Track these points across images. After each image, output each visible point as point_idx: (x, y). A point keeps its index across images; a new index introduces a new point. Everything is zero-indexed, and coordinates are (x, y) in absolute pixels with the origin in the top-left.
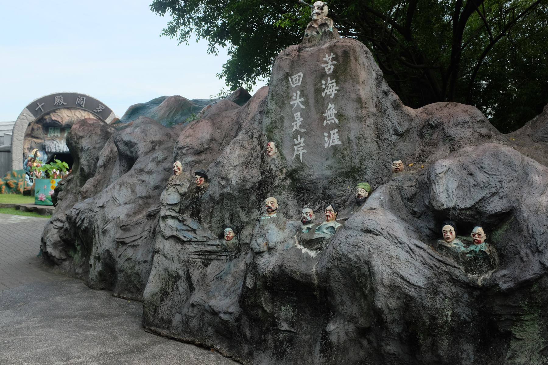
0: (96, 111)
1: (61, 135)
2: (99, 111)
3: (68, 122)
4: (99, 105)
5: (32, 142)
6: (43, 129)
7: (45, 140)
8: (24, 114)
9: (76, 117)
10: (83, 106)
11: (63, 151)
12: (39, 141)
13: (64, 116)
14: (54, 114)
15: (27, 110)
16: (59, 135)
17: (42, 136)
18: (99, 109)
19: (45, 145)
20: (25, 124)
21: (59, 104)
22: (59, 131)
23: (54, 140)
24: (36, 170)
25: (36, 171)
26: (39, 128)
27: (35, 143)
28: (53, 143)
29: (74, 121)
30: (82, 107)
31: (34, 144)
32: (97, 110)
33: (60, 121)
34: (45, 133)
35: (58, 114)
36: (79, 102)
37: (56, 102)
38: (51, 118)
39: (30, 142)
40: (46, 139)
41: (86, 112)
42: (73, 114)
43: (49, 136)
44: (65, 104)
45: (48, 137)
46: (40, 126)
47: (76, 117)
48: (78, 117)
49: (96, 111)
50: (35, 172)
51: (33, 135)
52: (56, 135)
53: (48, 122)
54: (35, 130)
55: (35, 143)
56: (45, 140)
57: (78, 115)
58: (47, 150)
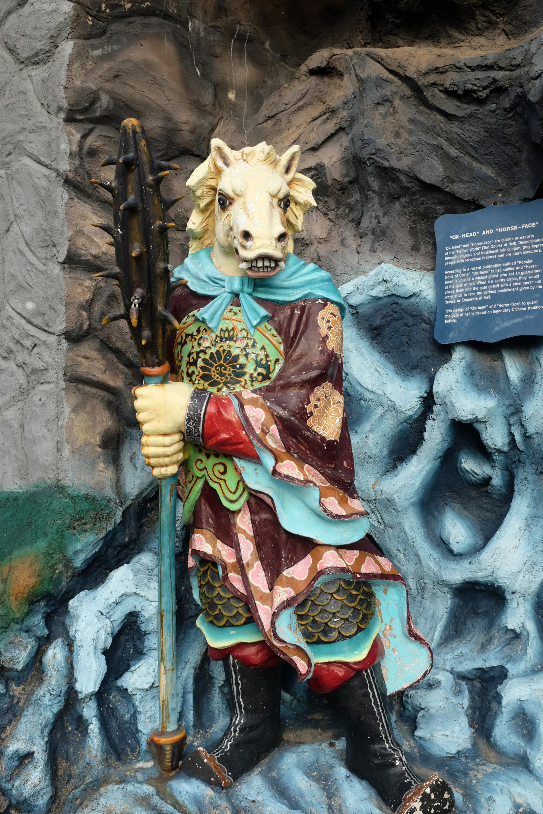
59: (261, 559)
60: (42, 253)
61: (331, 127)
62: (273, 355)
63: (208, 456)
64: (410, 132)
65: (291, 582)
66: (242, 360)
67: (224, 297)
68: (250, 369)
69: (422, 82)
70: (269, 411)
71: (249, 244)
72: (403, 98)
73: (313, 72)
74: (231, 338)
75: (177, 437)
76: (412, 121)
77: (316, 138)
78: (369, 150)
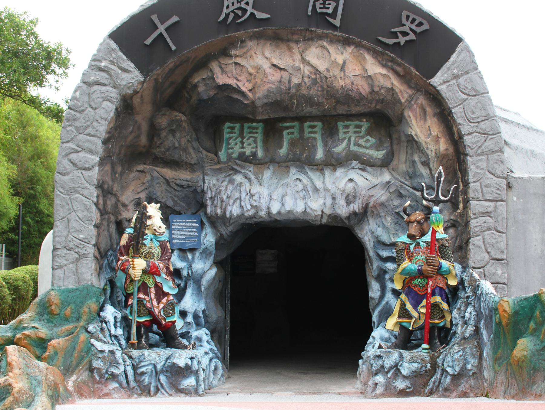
0: (391, 41)
1: (266, 149)
2: (402, 40)
3: (279, 89)
4: (405, 13)
5: (153, 178)
6: (196, 130)
7: (204, 174)
8: (103, 64)
9: (307, 70)
10: (337, 22)
11: (269, 213)
12: (183, 176)
13: (258, 68)
14: (225, 61)
15: (114, 46)
16: (260, 153)
17: (193, 157)
18: (405, 34)
19: (203, 192)
20: (106, 104)
21: (237, 17)
22: (259, 136)
23: (236, 172)
24: (144, 288)
25: (147, 293)
26: (179, 123)
27: (168, 182)
28: (231, 181)
29: (299, 85)
30: (334, 27)
31: (164, 187)
32: (395, 35)
33: (243, 89)
34: (208, 144)
35: (238, 60)
36: (318, 5)
37: (225, 11)
38: (213, 79)
39: (148, 178)
40: (207, 169)
41: (350, 49)
42: (298, 57)
43: (222, 155)
44: (260, 15)
45: (219, 162)
46: (183, 118)
47: (307, 70)
48: (317, 71)
49: (391, 41)
50: (141, 296)
51: (156, 151)
52: (248, 151)
53: (205, 97)
54: (163, 134)
55: (168, 182)
56: (204, 174)
57: (314, 61)
58: (209, 210)
59: (156, 298)
60: (87, 222)
61: (143, 188)
62: (160, 253)
63: (145, 275)
64: (165, 192)
65: (163, 303)
66: (154, 254)
67: (150, 239)
68: (156, 256)
69: (170, 181)
70: (163, 265)
71: (160, 229)
72: (163, 183)
73: (137, 171)
74: (151, 249)
75: (141, 271)
76: (166, 189)
77: (139, 190)
78: (155, 196)
